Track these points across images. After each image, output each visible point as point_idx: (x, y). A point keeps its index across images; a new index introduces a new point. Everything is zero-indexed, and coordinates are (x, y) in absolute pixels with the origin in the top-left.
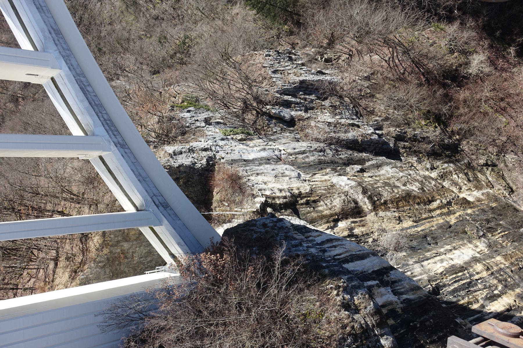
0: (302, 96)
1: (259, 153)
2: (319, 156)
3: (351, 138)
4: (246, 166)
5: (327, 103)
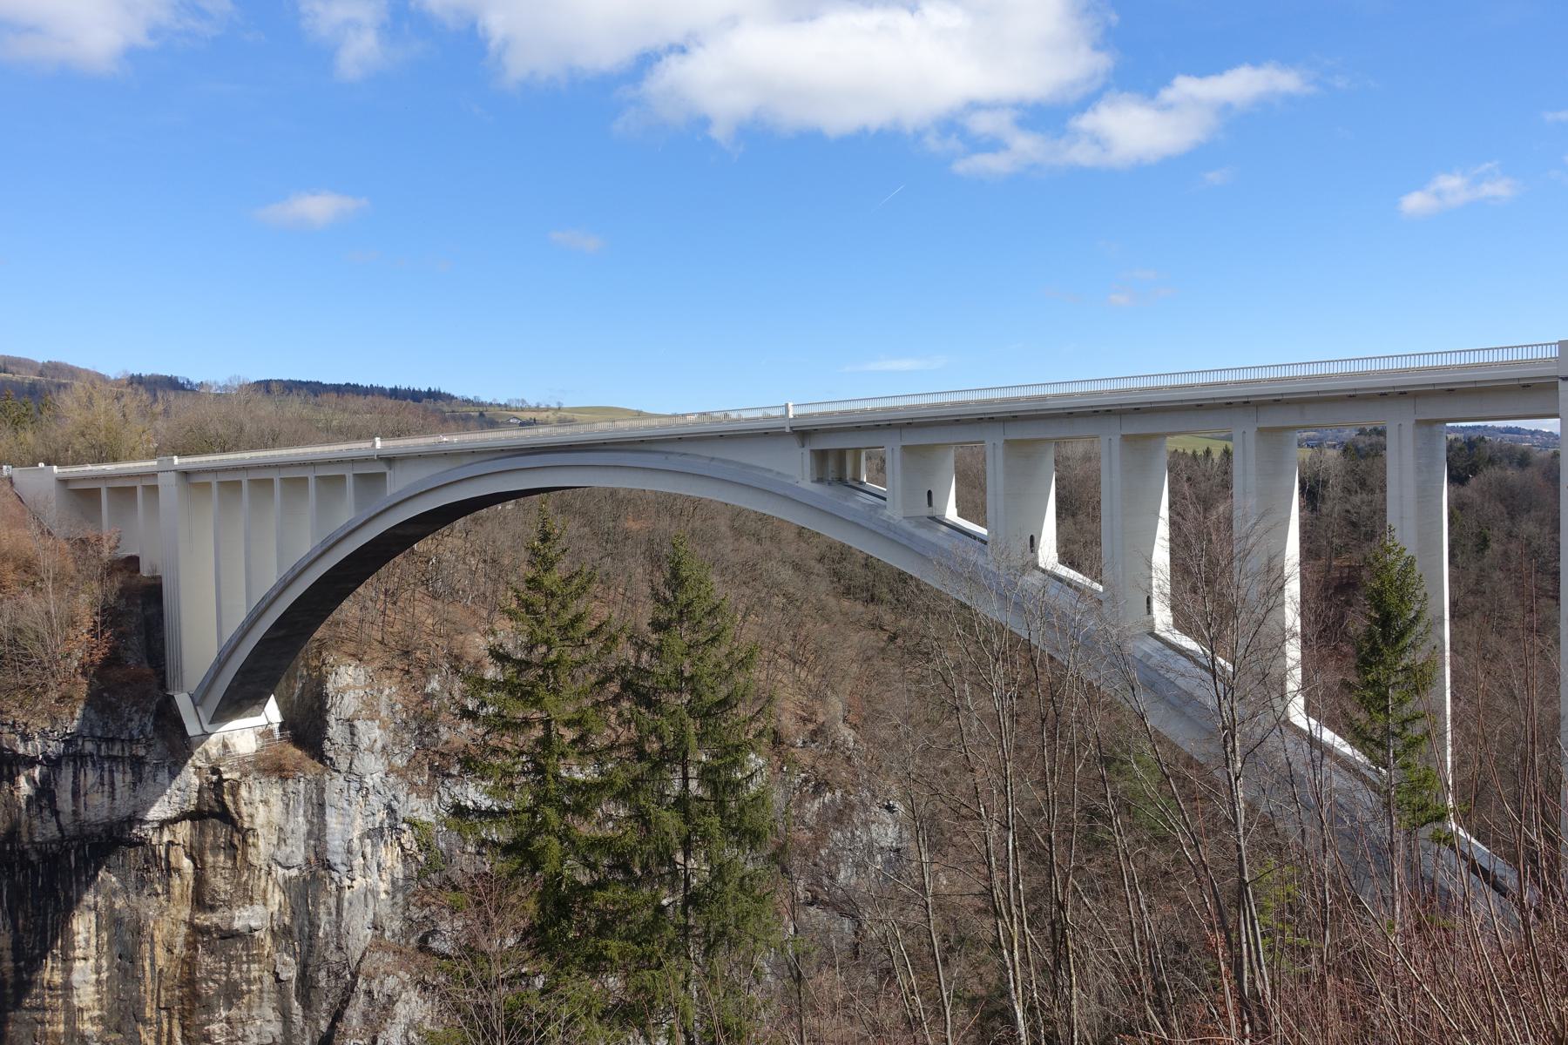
1: (338, 836)
2: (326, 935)
3: (348, 1012)
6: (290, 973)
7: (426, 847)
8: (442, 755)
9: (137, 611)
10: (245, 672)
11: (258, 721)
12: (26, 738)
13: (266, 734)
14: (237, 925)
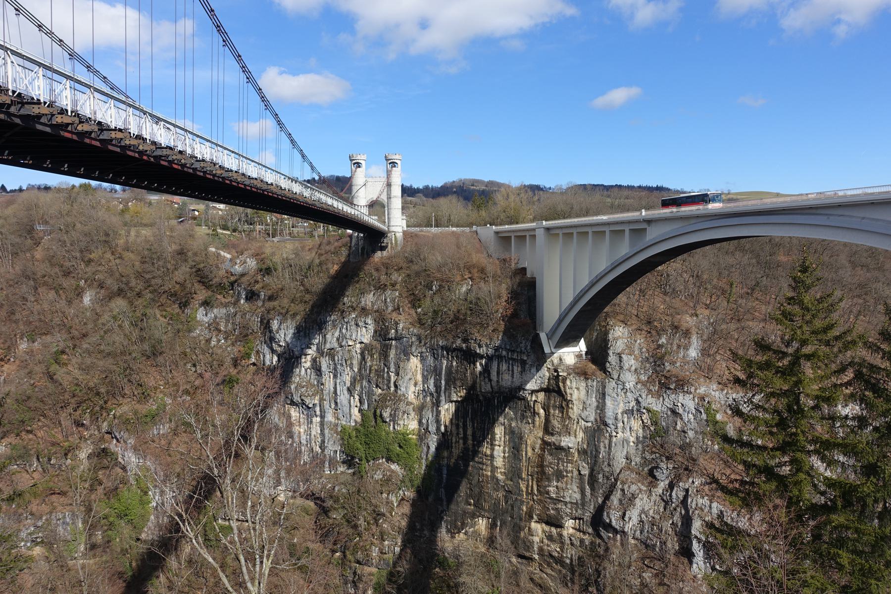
0: (679, 510)
3: (612, 497)
4: (598, 391)
5: (667, 525)
6: (586, 472)
7: (655, 423)
8: (666, 377)
9: (526, 291)
10: (571, 325)
11: (576, 349)
12: (480, 346)
13: (579, 356)
14: (563, 444)
